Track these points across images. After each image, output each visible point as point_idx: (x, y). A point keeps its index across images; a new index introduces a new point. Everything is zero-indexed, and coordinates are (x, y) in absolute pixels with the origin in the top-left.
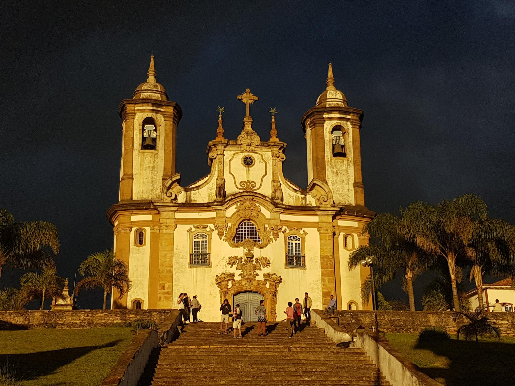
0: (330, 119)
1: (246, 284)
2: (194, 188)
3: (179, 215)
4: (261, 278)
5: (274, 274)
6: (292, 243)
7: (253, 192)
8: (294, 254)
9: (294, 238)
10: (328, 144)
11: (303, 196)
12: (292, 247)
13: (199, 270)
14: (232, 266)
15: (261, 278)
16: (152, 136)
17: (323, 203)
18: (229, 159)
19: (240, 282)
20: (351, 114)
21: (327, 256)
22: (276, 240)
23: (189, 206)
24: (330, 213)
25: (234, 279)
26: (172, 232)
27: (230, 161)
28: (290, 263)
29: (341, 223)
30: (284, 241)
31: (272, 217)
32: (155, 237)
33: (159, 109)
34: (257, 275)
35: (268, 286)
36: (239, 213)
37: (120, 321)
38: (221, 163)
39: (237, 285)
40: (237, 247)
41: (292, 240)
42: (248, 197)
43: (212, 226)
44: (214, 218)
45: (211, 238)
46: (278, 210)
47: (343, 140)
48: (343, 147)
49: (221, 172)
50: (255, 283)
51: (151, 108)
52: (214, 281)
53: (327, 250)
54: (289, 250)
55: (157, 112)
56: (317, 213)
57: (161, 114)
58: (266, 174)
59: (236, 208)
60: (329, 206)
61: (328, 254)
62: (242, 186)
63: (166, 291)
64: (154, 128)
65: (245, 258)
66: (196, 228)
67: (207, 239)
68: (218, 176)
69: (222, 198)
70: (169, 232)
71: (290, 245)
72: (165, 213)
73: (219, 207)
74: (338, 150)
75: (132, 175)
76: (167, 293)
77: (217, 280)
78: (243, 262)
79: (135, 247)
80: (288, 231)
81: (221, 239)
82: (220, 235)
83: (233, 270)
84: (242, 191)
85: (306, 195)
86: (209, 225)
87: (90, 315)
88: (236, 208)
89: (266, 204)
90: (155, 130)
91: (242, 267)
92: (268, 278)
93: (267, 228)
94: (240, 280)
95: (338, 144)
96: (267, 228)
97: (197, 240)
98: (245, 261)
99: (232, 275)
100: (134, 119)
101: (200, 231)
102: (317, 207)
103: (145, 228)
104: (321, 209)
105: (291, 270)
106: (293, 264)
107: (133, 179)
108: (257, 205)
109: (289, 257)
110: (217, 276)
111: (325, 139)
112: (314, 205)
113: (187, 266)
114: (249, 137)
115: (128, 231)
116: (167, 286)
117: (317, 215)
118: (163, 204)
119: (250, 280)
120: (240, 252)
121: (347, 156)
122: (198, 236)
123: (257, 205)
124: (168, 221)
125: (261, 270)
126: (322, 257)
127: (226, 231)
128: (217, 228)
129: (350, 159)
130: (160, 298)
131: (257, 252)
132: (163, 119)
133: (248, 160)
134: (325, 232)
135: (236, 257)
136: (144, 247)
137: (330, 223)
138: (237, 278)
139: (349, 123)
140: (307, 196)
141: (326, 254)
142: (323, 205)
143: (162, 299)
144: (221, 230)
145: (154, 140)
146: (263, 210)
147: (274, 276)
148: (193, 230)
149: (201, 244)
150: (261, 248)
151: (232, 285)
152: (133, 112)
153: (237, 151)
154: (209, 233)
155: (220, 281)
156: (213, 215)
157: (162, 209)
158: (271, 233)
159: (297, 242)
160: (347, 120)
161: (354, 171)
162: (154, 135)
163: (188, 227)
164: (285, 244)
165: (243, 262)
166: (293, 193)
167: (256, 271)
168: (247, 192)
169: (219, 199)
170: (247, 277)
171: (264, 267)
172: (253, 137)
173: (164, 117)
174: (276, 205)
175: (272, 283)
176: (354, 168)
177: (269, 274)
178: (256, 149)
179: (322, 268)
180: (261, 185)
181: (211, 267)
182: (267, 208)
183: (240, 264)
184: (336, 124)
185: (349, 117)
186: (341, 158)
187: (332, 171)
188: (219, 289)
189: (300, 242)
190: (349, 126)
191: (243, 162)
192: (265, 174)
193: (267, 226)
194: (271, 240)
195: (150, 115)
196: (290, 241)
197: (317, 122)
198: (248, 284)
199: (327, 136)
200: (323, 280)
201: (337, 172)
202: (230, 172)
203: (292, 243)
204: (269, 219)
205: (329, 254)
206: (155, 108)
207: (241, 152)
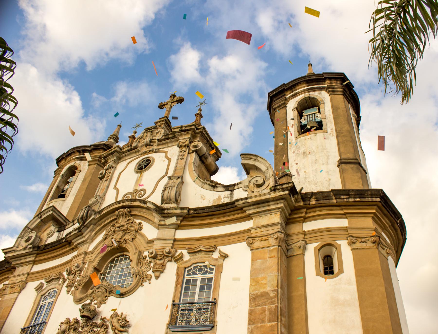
11: (229, 192)
17: (256, 190)
21: (264, 295)
24: (273, 207)
27: (121, 173)
31: (161, 237)
41: (194, 274)
53: (264, 282)
56: (248, 212)
60: (268, 191)
61: (268, 289)
80: (187, 257)
89: (150, 217)
108: (137, 221)
117: (249, 217)
118: (16, 254)
129: (329, 131)
141: (262, 290)
150: (122, 295)
157: (17, 262)
161: (338, 144)
172: (155, 134)
176: (338, 140)
179: (251, 322)
180: (153, 192)
192: (164, 174)
197: (277, 106)
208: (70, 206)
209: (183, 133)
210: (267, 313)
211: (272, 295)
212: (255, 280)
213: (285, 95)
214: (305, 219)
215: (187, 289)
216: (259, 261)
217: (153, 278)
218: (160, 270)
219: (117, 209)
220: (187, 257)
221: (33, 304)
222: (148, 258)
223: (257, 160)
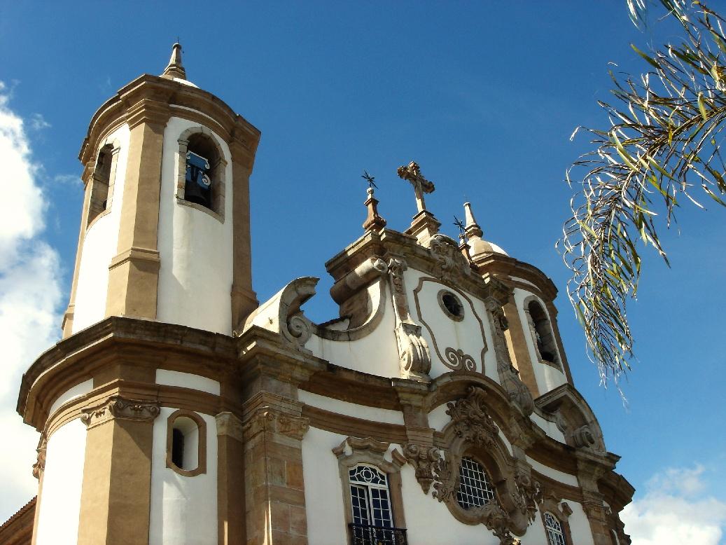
26: (294, 443)
27: (416, 292)
36: (459, 428)
42: (479, 389)
45: (400, 485)
59: (448, 413)
66: (355, 448)
72: (274, 382)
81: (426, 491)
82: (423, 479)
86: (393, 446)
89: (506, 421)
90: (208, 172)
101: (365, 460)
115: (146, 414)
117: (573, 471)
148: (348, 450)
154: (392, 470)
156: (393, 417)
162: (206, 181)
163: (339, 438)
195: (207, 131)
207: (433, 280)
209: (496, 291)
221: (339, 481)
223: (581, 403)
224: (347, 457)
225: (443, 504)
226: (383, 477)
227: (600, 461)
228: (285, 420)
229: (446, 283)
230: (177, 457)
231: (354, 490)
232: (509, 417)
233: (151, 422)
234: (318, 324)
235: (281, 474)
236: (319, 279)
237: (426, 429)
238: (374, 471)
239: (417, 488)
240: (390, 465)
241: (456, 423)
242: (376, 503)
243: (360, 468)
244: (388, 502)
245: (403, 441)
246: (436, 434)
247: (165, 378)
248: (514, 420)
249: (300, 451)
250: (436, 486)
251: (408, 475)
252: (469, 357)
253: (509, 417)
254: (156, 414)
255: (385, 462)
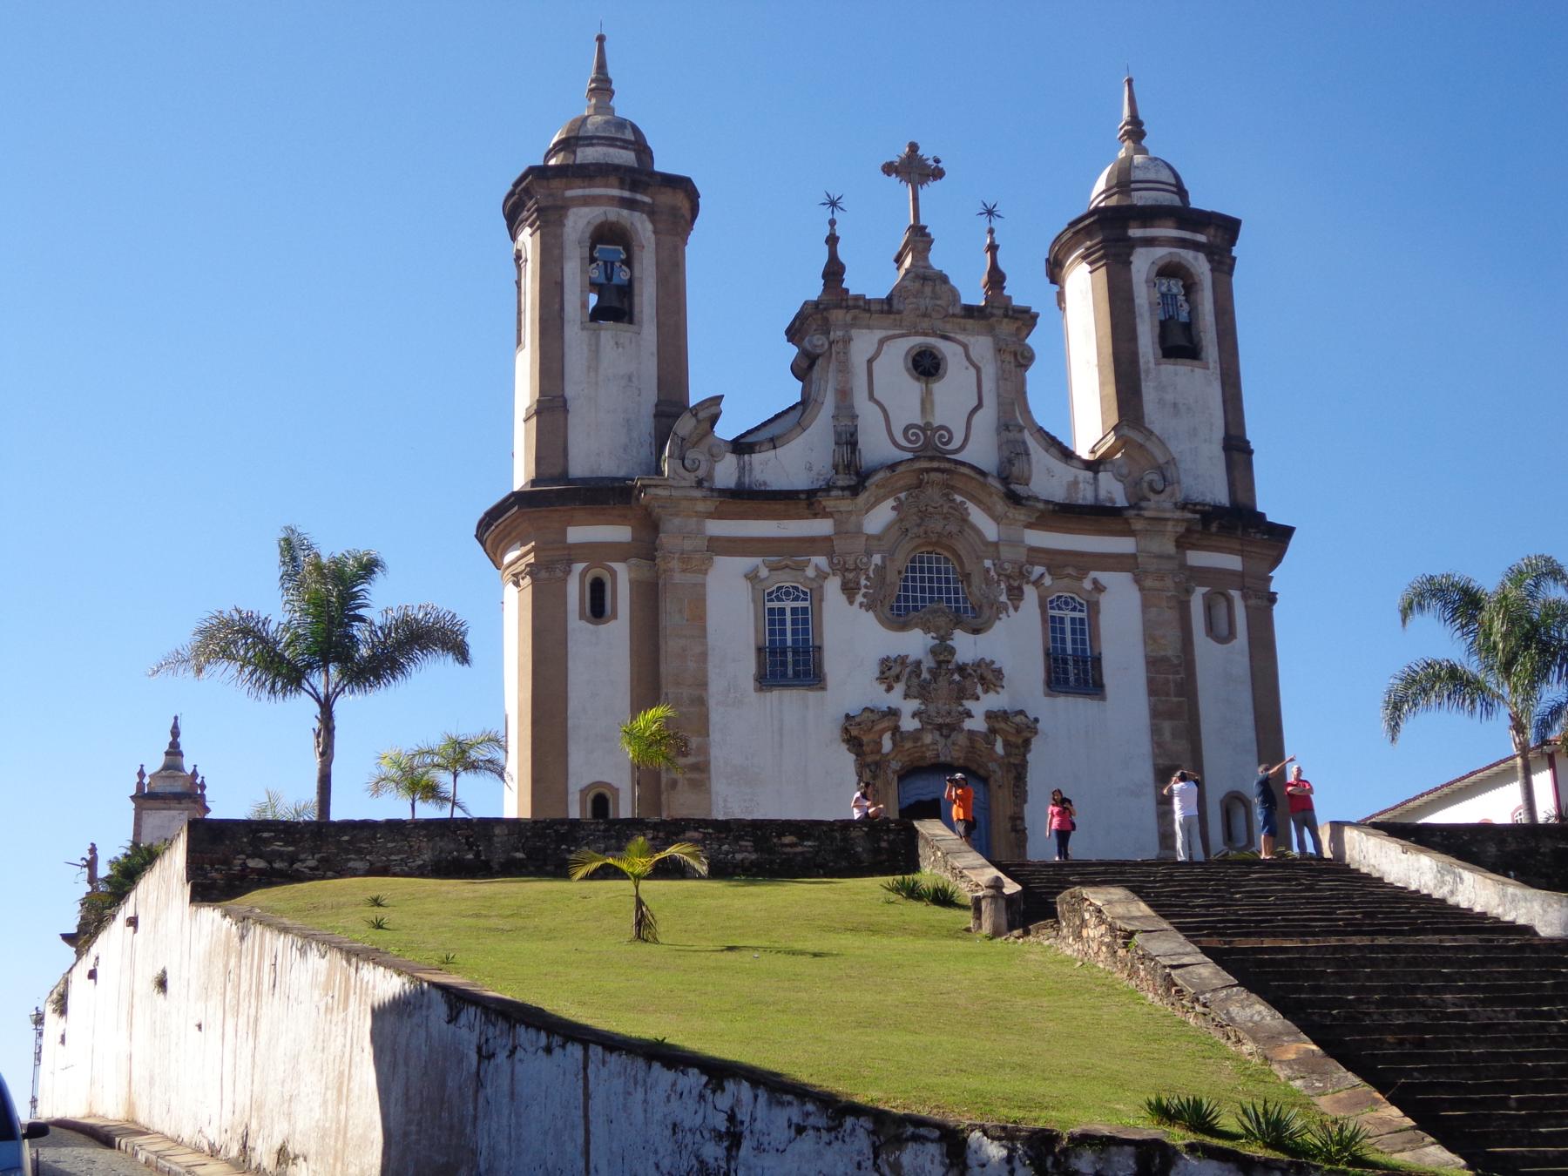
0: (1150, 242)
1: (935, 743)
2: (761, 443)
3: (719, 528)
4: (977, 724)
5: (1021, 712)
6: (1062, 620)
7: (949, 460)
8: (1070, 651)
9: (1066, 603)
10: (1146, 315)
11: (1089, 474)
12: (1063, 631)
13: (789, 701)
14: (889, 689)
15: (977, 724)
16: (615, 281)
17: (1152, 496)
18: (868, 356)
19: (916, 736)
20: (1212, 231)
21: (1165, 659)
22: (1016, 609)
23: (748, 498)
25: (896, 730)
27: (870, 362)
28: (1057, 679)
29: (1197, 558)
30: (1038, 611)
32: (649, 596)
33: (639, 197)
34: (969, 715)
35: (999, 748)
37: (754, 857)
38: (845, 368)
39: (908, 745)
40: (904, 627)
43: (821, 561)
44: (828, 539)
45: (821, 600)
46: (1020, 515)
47: (1186, 307)
48: (1189, 328)
49: (844, 395)
50: (962, 740)
51: (616, 192)
52: (837, 733)
54: (1054, 640)
55: (630, 204)
57: (643, 212)
58: (979, 406)
59: (894, 508)
60: (1168, 505)
61: (1170, 653)
62: (909, 441)
63: (691, 760)
64: (623, 256)
65: (928, 663)
66: (772, 569)
67: (806, 604)
68: (837, 408)
69: (853, 475)
70: (690, 578)
71: (1053, 626)
72: (677, 521)
73: (845, 505)
74: (1179, 340)
75: (565, 401)
76: (696, 768)
77: (846, 730)
78: (925, 675)
79: (584, 624)
80: (1048, 581)
81: (851, 603)
82: (849, 590)
83: (895, 699)
84: (910, 455)
85: (1096, 472)
87: (661, 835)
88: (894, 508)
91: (921, 690)
92: (1003, 725)
93: (988, 571)
94: (916, 730)
95: (1171, 318)
96: (988, 571)
97: (776, 605)
98: (930, 670)
99: (893, 713)
100: (562, 225)
102: (1131, 507)
103: (614, 565)
104: (1146, 514)
105: (1062, 701)
106: (1067, 681)
107: (566, 410)
108: (959, 498)
109: (1056, 660)
110: (847, 716)
111: (1137, 301)
112: (1121, 501)
113: (749, 683)
114: (928, 290)
115: (559, 574)
116: (694, 742)
117: (1130, 533)
119: (948, 729)
120: (915, 643)
121: (1203, 355)
122: (781, 593)
123: (959, 498)
124: (688, 545)
125: (978, 699)
126: (1153, 663)
127: (868, 578)
128: (839, 568)
129: (1211, 365)
130: (673, 784)
131: (967, 647)
132: (649, 226)
133: (927, 363)
134: (1157, 584)
135: (902, 660)
136: (612, 624)
137: (1169, 557)
138: (909, 724)
139: (1201, 256)
140: (1101, 475)
142: (1152, 504)
143: (679, 787)
144: (850, 576)
145: (627, 291)
146: (977, 516)
147: (1018, 719)
148: (764, 573)
149: (788, 617)
150: (976, 631)
151: (894, 744)
152: (560, 203)
153: (891, 333)
154: (815, 585)
155: (858, 734)
156: (820, 527)
158: (1003, 586)
159: (1077, 615)
160: (1196, 246)
161: (1225, 402)
162: (622, 276)
164: (1044, 621)
165: (925, 675)
166: (1058, 466)
167: (965, 702)
168: (932, 459)
169: (842, 481)
170: (940, 721)
171: (986, 691)
173: (653, 222)
174: (1014, 499)
175: (1012, 739)
177: (1005, 712)
178: (948, 327)
181: (823, 688)
182: (989, 510)
183: (915, 681)
184: (1167, 260)
185: (1202, 238)
186: (1188, 361)
187: (1161, 402)
188: (853, 757)
189: (1084, 615)
190: (1200, 266)
191: (910, 365)
192: (975, 403)
193: (988, 563)
194: (1002, 608)
195: (615, 214)
196: (1056, 613)
198: (942, 741)
199: (1143, 296)
200: (1155, 731)
201: (1175, 405)
202: (871, 397)
203: (1062, 620)
204: (996, 545)
205: (1171, 650)
206: (626, 194)
208: (654, 350)
210: (1172, 685)
211: (1176, 662)
212: (1149, 636)
213: (1126, 228)
214: (1195, 547)
215: (1054, 630)
216: (1154, 610)
217: (1011, 610)
218: (1016, 594)
219: (928, 470)
220: (1048, 581)
222: (992, 573)
224: (762, 580)
225: (871, 613)
226: (805, 593)
227: (1168, 515)
228: (685, 558)
229: (917, 334)
230: (598, 608)
231: (771, 611)
232: (991, 495)
233: (565, 581)
234: (730, 438)
235: (680, 611)
236: (718, 400)
237: (859, 531)
238: (796, 588)
239: (843, 598)
240: (813, 580)
241: (901, 520)
242: (794, 622)
243: (779, 588)
244: (807, 620)
245: (830, 554)
246: (869, 537)
247: (577, 534)
248: (996, 498)
249: (704, 585)
250: (865, 596)
251: (833, 586)
252: (942, 427)
253: (991, 495)
254: (568, 572)
255: (807, 578)
